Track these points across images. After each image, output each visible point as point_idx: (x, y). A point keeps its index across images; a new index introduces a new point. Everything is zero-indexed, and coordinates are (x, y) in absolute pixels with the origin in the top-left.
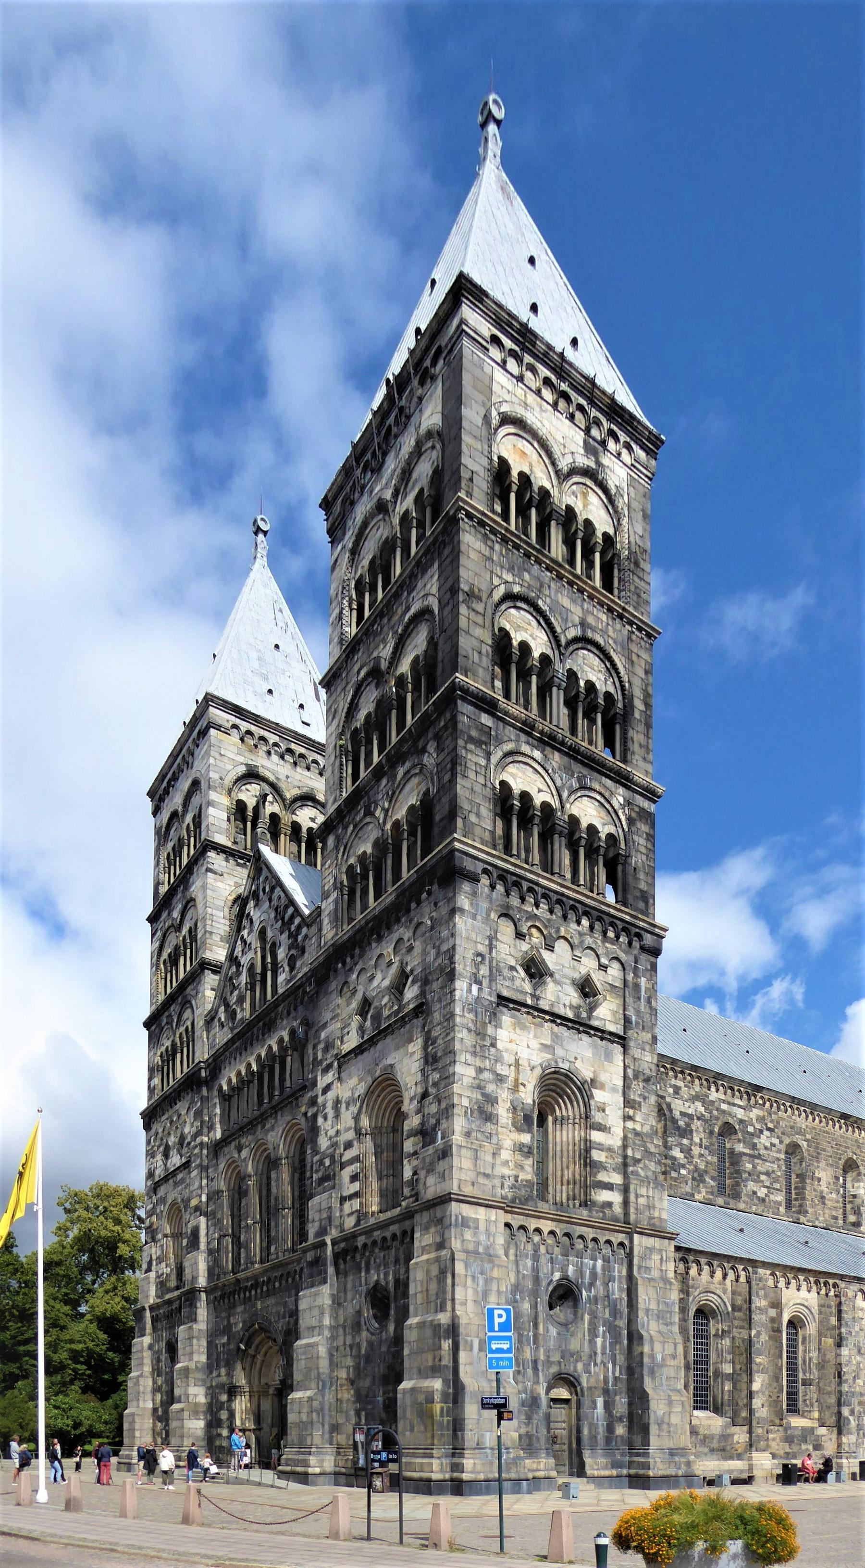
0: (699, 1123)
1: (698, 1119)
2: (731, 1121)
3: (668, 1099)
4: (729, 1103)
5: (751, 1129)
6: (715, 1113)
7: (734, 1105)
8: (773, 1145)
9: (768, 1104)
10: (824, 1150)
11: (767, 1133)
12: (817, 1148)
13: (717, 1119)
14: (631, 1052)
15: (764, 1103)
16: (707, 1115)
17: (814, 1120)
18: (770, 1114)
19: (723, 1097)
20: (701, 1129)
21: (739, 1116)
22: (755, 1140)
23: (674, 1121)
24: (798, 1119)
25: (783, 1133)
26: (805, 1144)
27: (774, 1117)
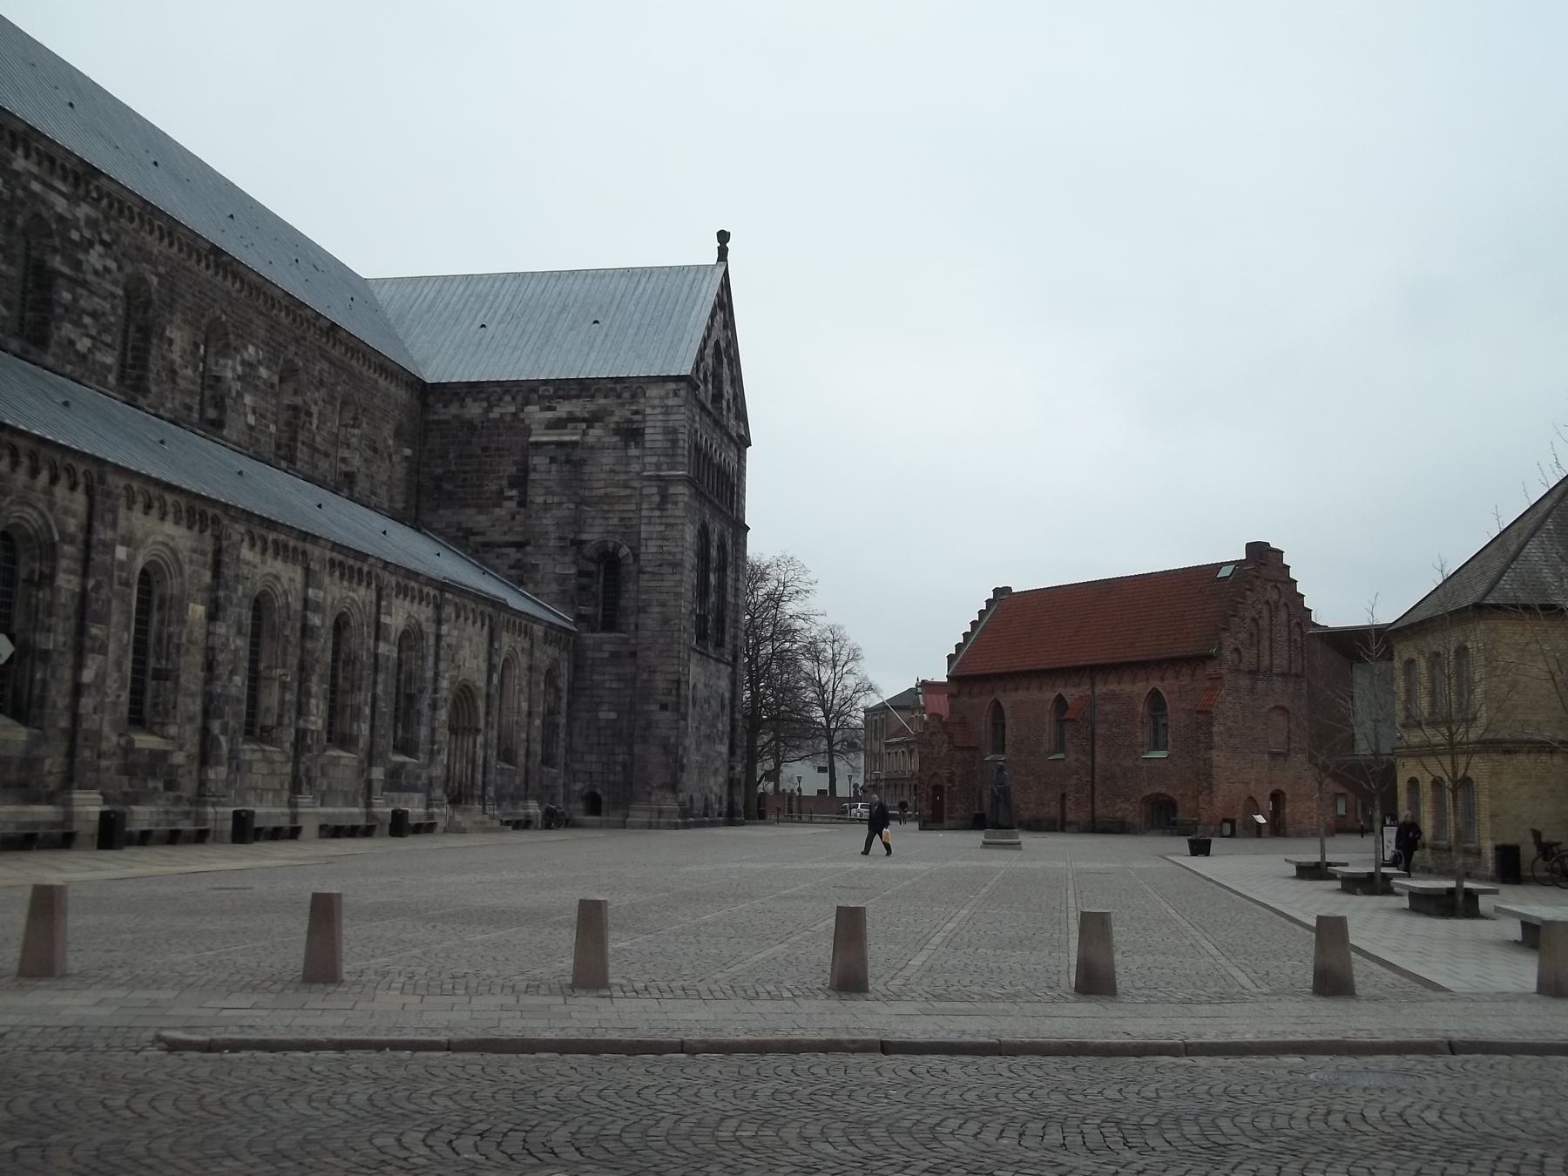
2: (45, 213)
4: (44, 183)
5: (75, 235)
6: (20, 193)
7: (53, 188)
8: (107, 270)
9: (105, 202)
10: (182, 297)
11: (99, 248)
13: (22, 203)
15: (99, 199)
17: (171, 244)
19: (35, 170)
21: (59, 210)
22: (81, 256)
24: (149, 239)
26: (155, 280)
27: (113, 224)
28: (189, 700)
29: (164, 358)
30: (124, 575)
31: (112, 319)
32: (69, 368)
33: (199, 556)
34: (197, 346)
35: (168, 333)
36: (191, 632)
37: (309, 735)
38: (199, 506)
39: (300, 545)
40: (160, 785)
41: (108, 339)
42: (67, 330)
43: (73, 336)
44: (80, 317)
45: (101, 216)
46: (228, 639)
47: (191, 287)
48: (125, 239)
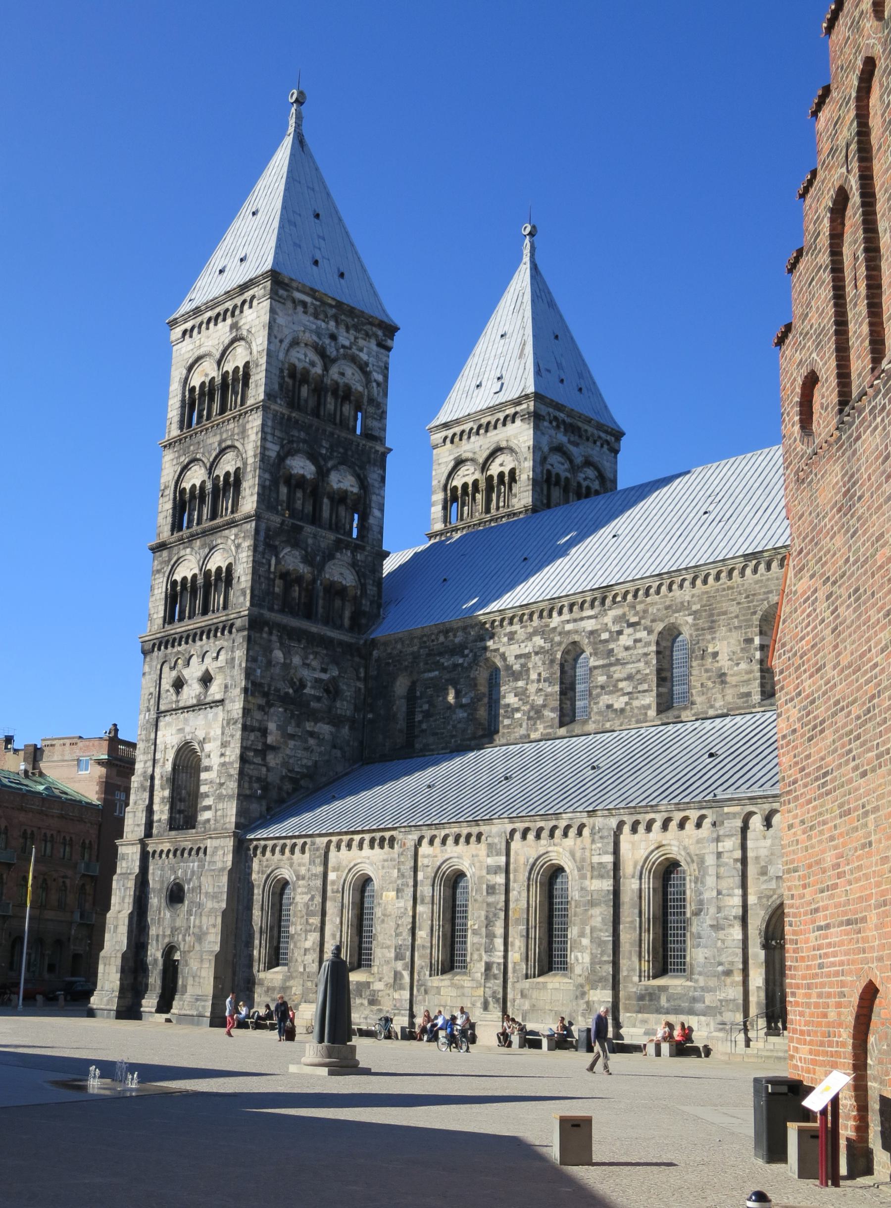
0: (537, 658)
1: (537, 653)
2: (577, 638)
3: (501, 650)
4: (575, 621)
5: (605, 636)
8: (636, 641)
12: (712, 615)
13: (560, 644)
14: (226, 708)
16: (547, 646)
18: (633, 607)
20: (540, 663)
21: (589, 629)
22: (611, 646)
23: (508, 668)
25: (653, 621)
26: (690, 619)
28: (385, 951)
29: (707, 671)
30: (335, 887)
31: (648, 671)
32: (608, 725)
33: (390, 863)
34: (749, 641)
35: (710, 650)
36: (385, 909)
37: (495, 966)
38: (378, 835)
39: (475, 830)
40: (366, 1002)
41: (645, 686)
42: (605, 699)
43: (610, 702)
44: (615, 686)
45: (627, 609)
46: (406, 909)
47: (733, 600)
48: (652, 610)
